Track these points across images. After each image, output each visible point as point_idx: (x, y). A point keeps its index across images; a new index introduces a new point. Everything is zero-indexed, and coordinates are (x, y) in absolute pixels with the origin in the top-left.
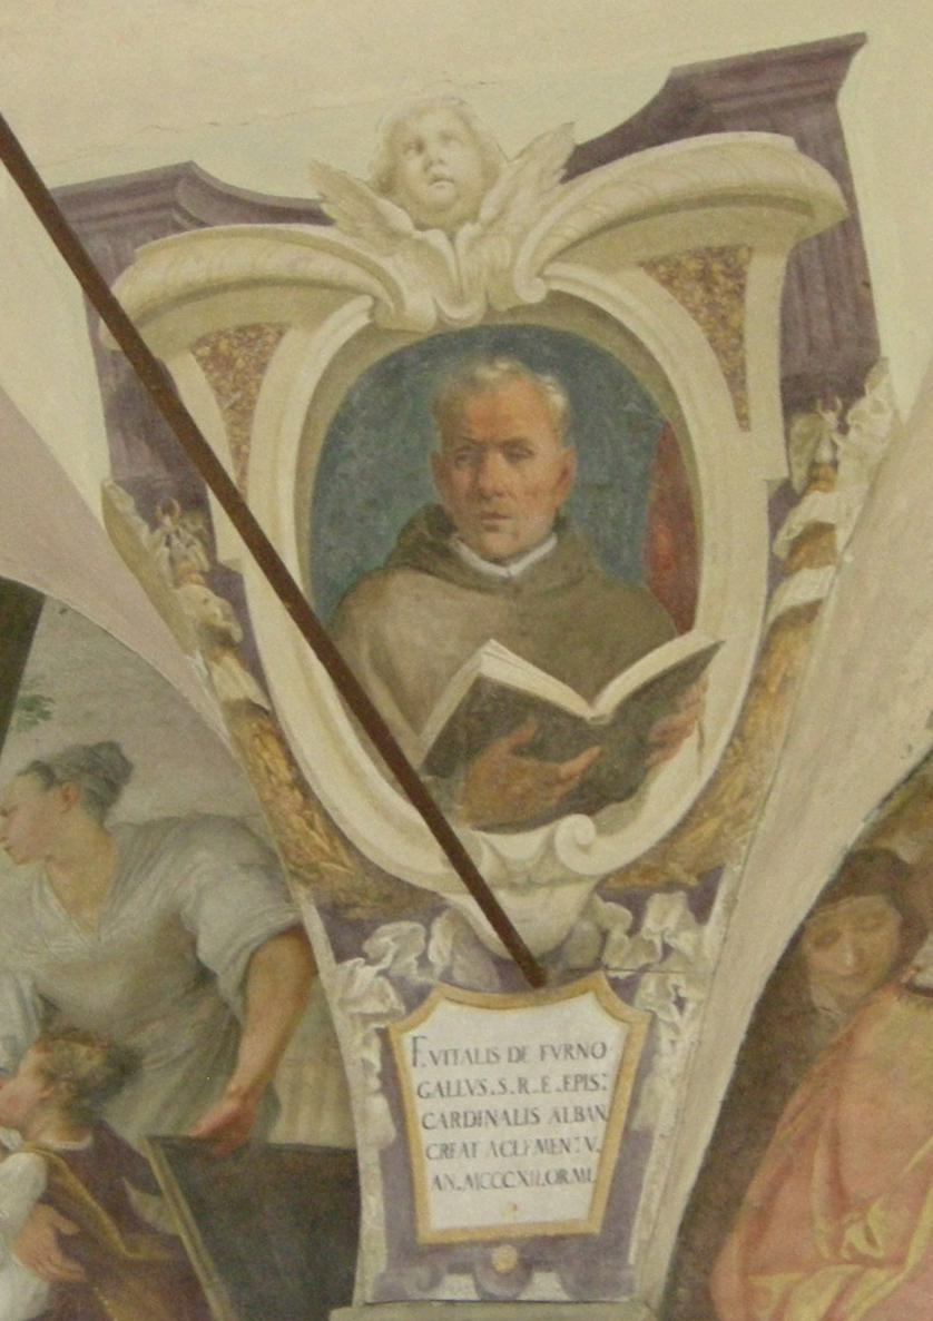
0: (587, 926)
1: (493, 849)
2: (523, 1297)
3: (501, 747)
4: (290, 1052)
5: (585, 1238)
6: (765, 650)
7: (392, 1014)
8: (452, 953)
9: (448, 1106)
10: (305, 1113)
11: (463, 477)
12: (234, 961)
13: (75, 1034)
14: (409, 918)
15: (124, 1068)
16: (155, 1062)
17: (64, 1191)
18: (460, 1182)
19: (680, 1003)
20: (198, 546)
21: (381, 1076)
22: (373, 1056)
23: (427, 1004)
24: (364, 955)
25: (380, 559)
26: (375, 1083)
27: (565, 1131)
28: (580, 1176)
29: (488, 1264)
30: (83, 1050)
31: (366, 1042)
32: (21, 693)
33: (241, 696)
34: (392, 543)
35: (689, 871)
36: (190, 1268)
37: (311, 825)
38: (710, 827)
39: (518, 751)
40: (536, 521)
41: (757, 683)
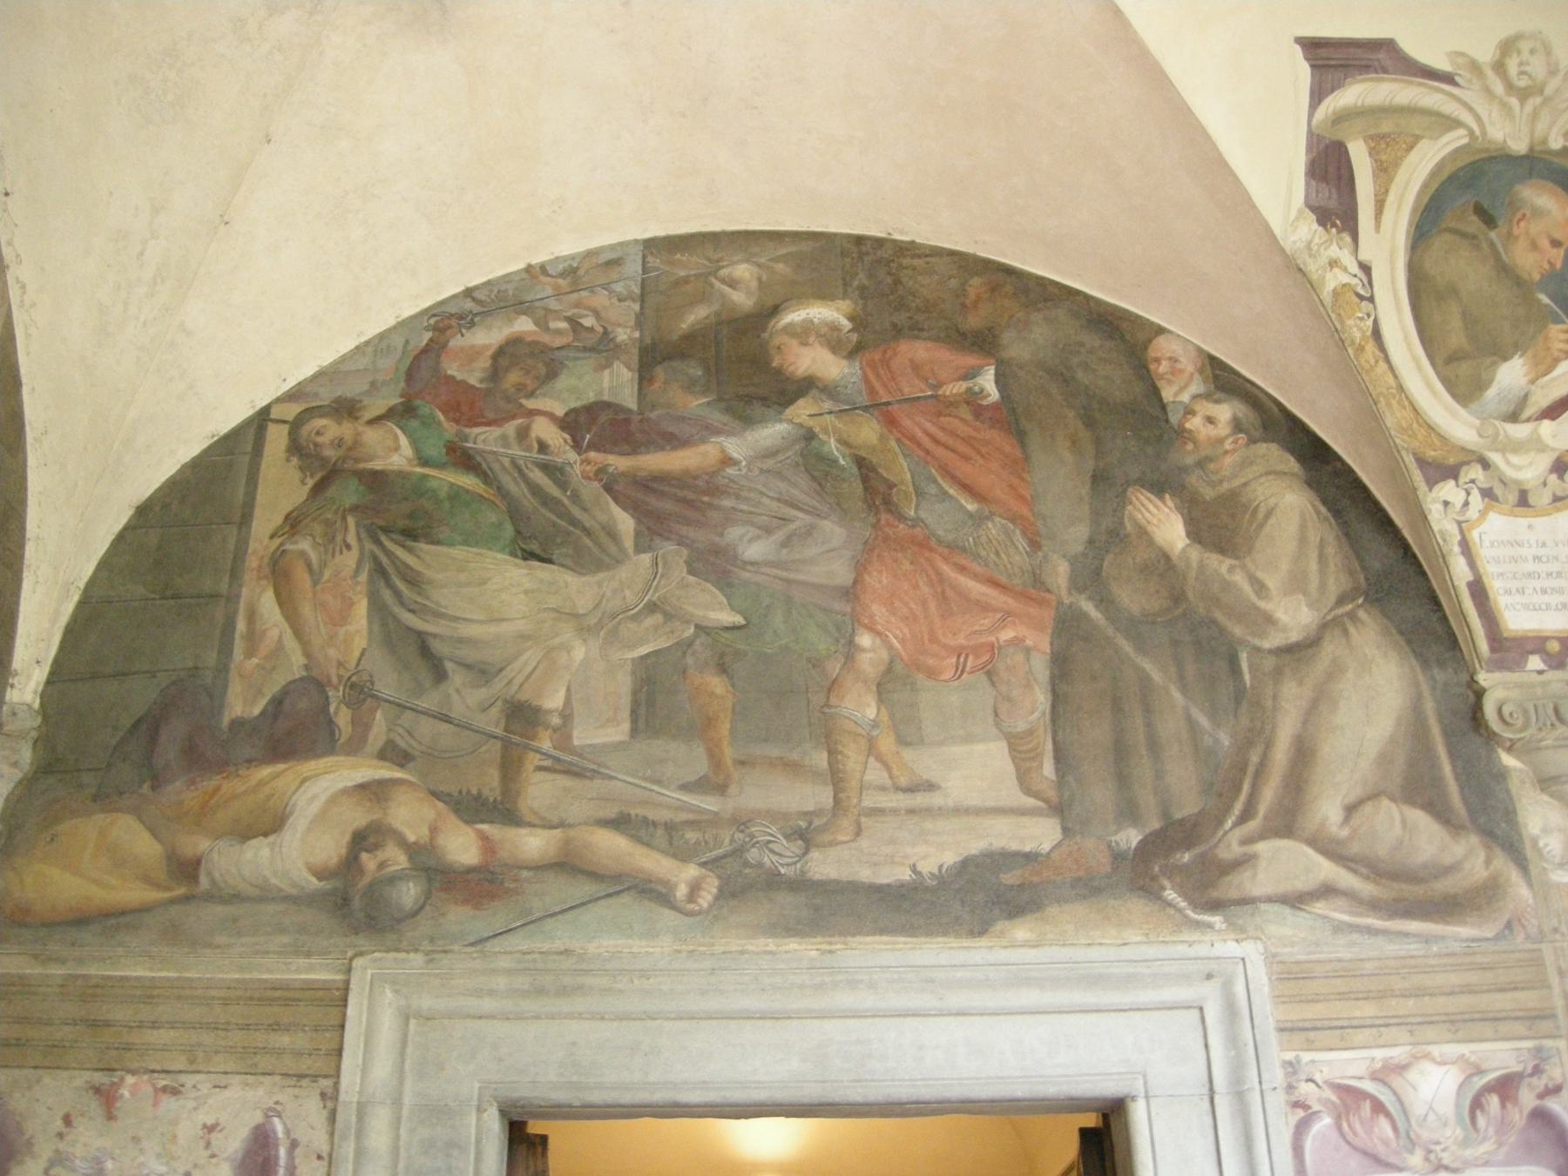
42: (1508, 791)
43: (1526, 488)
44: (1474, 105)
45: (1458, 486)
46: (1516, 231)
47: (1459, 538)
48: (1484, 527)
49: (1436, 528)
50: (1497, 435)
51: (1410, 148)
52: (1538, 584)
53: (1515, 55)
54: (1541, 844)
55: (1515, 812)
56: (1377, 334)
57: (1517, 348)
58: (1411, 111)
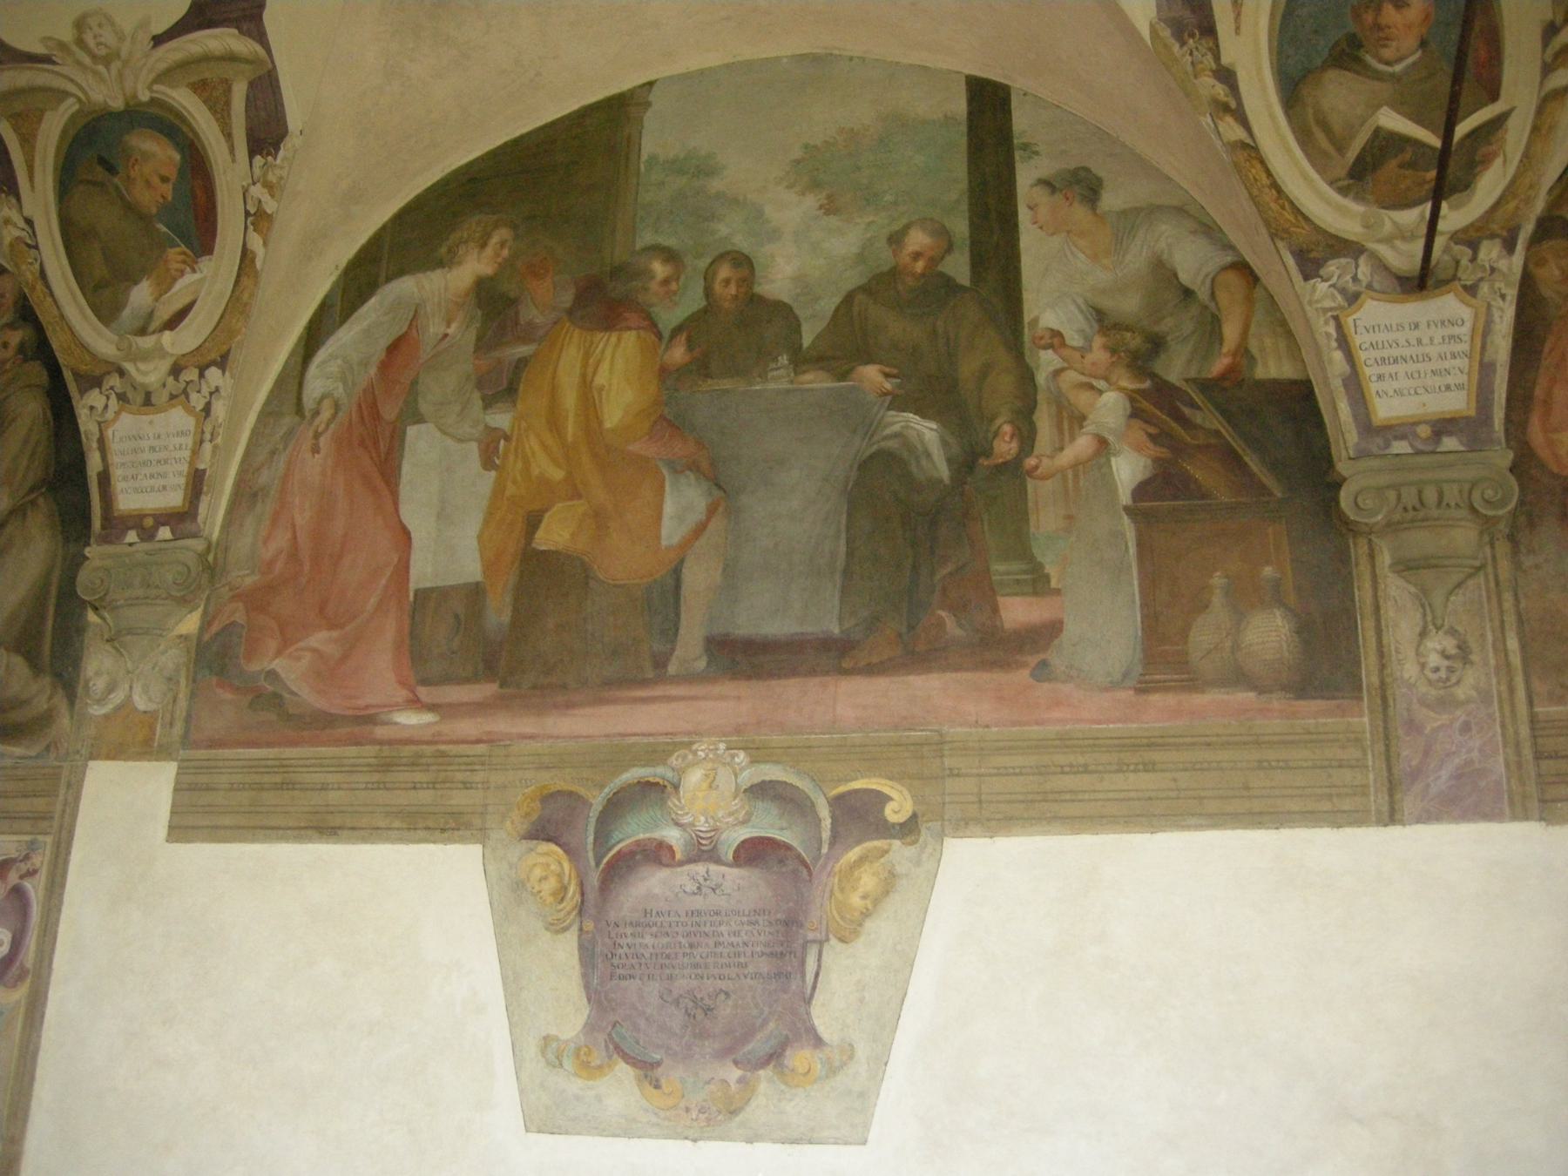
0: (1446, 258)
1: (1389, 218)
2: (1438, 450)
3: (1392, 164)
4: (1253, 330)
5: (1467, 418)
6: (1540, 111)
7: (1341, 308)
8: (1371, 275)
9: (1378, 354)
10: (1271, 363)
11: (1369, 18)
12: (1203, 282)
13: (1118, 327)
14: (1345, 256)
15: (1157, 344)
16: (1172, 340)
17: (1143, 411)
18: (1391, 393)
19: (1503, 297)
20: (1209, 57)
21: (1337, 340)
22: (1332, 329)
23: (1359, 301)
24: (1321, 277)
25: (1318, 62)
26: (1334, 344)
27: (1447, 364)
28: (1459, 387)
29: (1416, 435)
30: (1128, 335)
31: (1326, 323)
32: (1015, 141)
33: (1237, 138)
34: (1326, 53)
35: (1502, 228)
36: (1231, 446)
37: (1283, 208)
38: (1512, 205)
39: (1401, 166)
40: (1411, 42)
41: (1535, 129)
42: (82, 641)
43: (151, 389)
44: (72, 77)
45: (101, 393)
46: (132, 174)
47: (98, 436)
48: (117, 425)
49: (82, 429)
50: (130, 346)
51: (40, 120)
52: (147, 471)
53: (88, 30)
54: (91, 684)
55: (81, 659)
56: (43, 274)
57: (144, 272)
58: (32, 90)
